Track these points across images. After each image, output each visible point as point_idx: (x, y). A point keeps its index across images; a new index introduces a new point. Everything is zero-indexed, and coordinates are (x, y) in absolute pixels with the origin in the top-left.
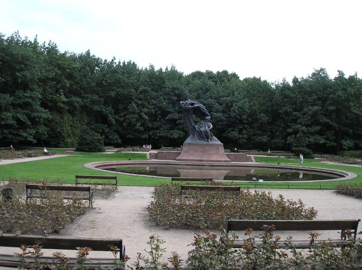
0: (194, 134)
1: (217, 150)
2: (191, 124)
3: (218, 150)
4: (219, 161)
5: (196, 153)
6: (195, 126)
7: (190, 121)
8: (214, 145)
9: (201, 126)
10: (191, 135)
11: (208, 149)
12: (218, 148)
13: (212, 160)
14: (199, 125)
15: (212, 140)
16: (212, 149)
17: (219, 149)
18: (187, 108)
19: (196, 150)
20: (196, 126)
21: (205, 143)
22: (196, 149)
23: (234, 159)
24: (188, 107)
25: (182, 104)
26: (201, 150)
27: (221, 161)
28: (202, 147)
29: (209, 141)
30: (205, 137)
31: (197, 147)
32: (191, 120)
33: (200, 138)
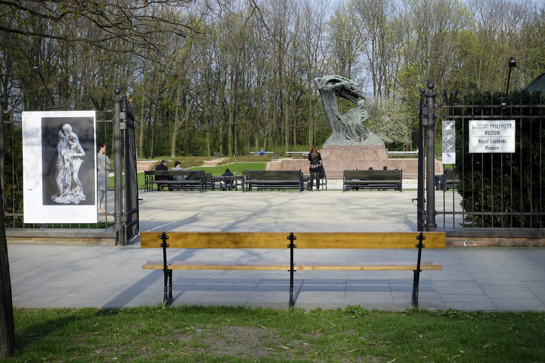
0: (338, 131)
1: (375, 155)
2: (334, 114)
3: (377, 155)
5: (341, 161)
6: (340, 117)
7: (332, 110)
8: (370, 148)
12: (376, 152)
16: (366, 154)
17: (379, 153)
18: (325, 89)
19: (340, 156)
20: (343, 118)
21: (357, 143)
22: (340, 154)
25: (317, 82)
26: (349, 155)
28: (350, 150)
29: (362, 140)
30: (355, 135)
32: (333, 107)
33: (347, 136)
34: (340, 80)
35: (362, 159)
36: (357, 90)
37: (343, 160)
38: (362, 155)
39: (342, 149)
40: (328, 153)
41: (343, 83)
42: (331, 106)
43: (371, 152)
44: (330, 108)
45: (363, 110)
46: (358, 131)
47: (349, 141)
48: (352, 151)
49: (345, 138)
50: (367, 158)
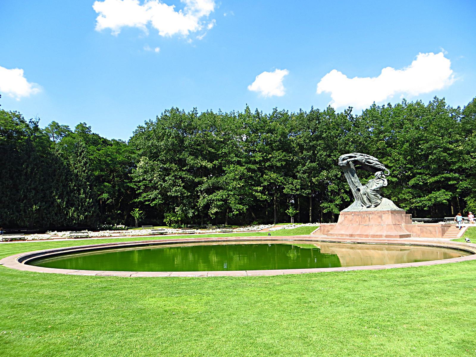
1: (380, 219)
3: (382, 220)
4: (377, 235)
9: (368, 186)
10: (355, 199)
11: (366, 218)
12: (381, 217)
13: (365, 235)
14: (367, 185)
15: (380, 205)
17: (383, 218)
19: (351, 221)
23: (419, 232)
24: (341, 164)
26: (357, 220)
27: (381, 236)
28: (358, 215)
29: (373, 206)
31: (353, 216)
32: (353, 180)
34: (356, 156)
35: (367, 223)
36: (374, 164)
37: (352, 224)
38: (368, 220)
39: (353, 214)
40: (343, 218)
41: (356, 159)
42: (351, 179)
43: (376, 217)
44: (350, 180)
45: (379, 180)
46: (369, 199)
47: (362, 207)
48: (359, 216)
49: (360, 205)
50: (372, 222)
